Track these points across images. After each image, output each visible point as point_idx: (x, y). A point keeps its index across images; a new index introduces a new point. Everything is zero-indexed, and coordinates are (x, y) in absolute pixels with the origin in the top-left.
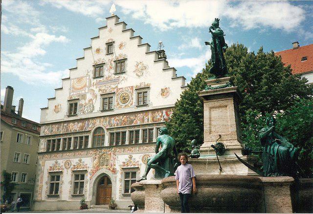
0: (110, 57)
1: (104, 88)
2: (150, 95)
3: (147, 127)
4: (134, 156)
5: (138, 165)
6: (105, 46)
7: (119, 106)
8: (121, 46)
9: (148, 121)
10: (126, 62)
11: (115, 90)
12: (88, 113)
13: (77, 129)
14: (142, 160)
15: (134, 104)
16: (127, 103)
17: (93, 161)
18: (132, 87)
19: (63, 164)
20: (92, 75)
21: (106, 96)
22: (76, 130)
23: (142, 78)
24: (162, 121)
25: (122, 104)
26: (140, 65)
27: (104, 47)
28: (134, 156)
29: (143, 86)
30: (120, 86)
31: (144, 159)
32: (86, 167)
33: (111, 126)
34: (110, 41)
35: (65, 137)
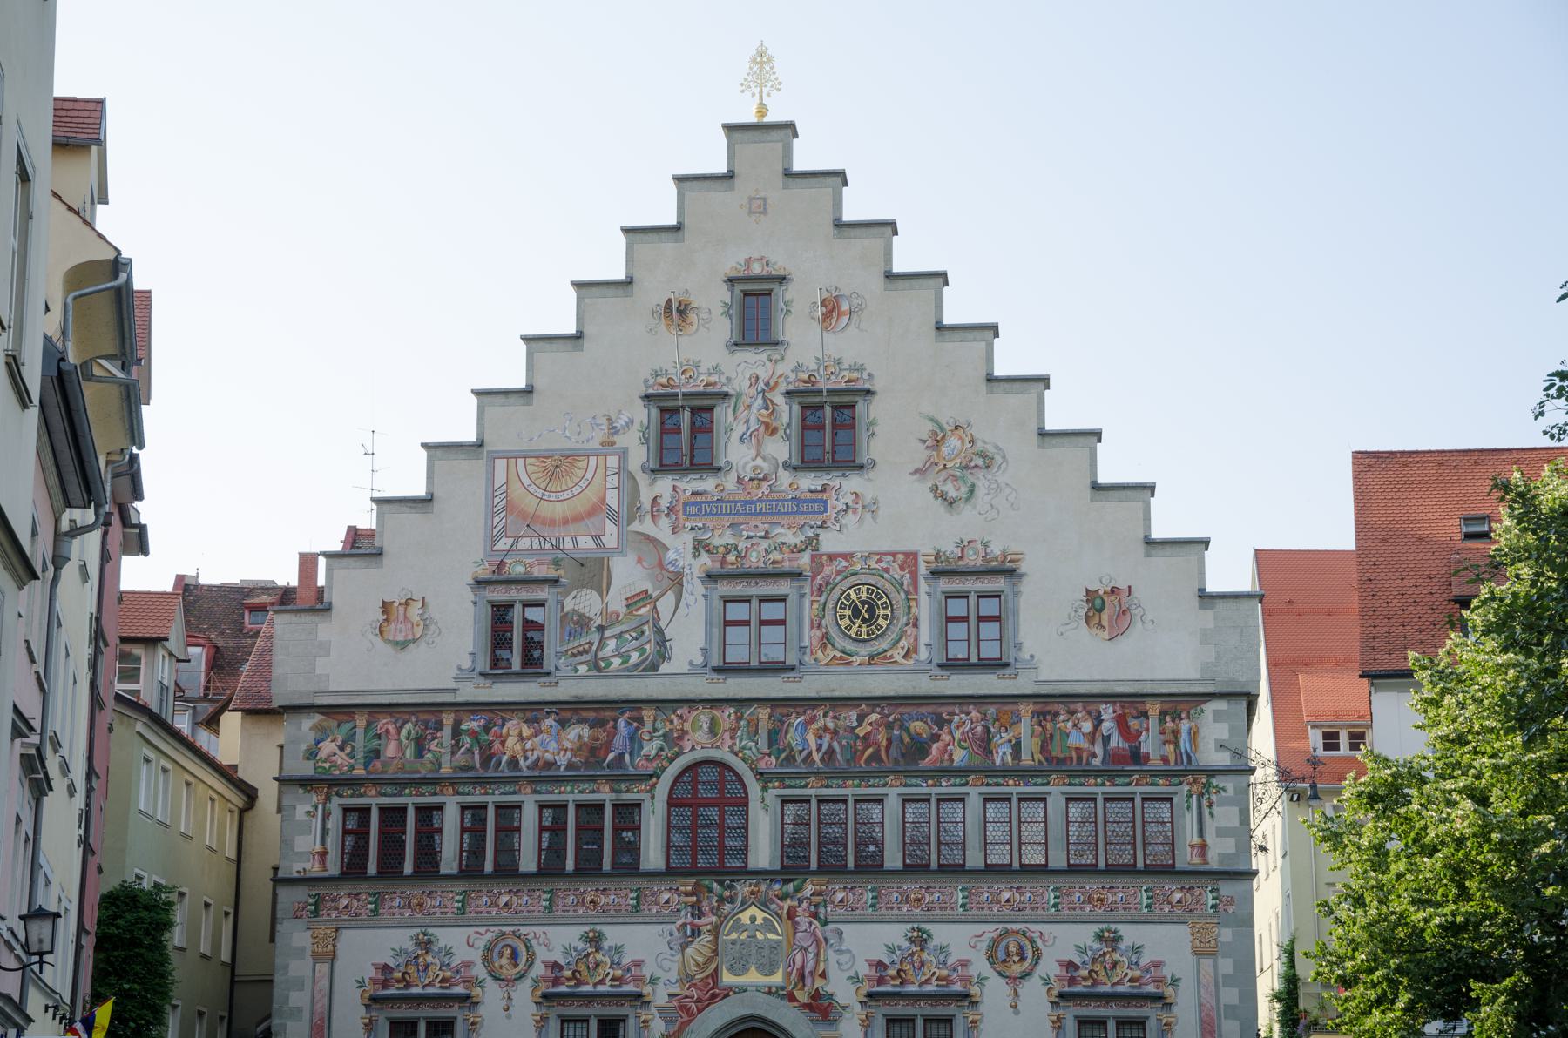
0: (754, 362)
1: (728, 538)
2: (1023, 616)
3: (1014, 789)
4: (941, 934)
5: (966, 980)
6: (724, 294)
7: (831, 652)
8: (830, 310)
9: (1017, 753)
10: (860, 407)
11: (805, 559)
12: (617, 675)
13: (562, 760)
14: (991, 956)
15: (923, 654)
16: (884, 644)
17: (684, 947)
18: (911, 557)
19: (476, 956)
20: (639, 455)
21: (739, 589)
22: (550, 765)
23: (967, 513)
24: (1097, 762)
25: (850, 646)
26: (953, 443)
27: (713, 301)
28: (941, 934)
29: (973, 559)
30: (830, 542)
31: (1001, 955)
32: (638, 980)
33: (790, 759)
34: (757, 269)
35: (476, 798)
